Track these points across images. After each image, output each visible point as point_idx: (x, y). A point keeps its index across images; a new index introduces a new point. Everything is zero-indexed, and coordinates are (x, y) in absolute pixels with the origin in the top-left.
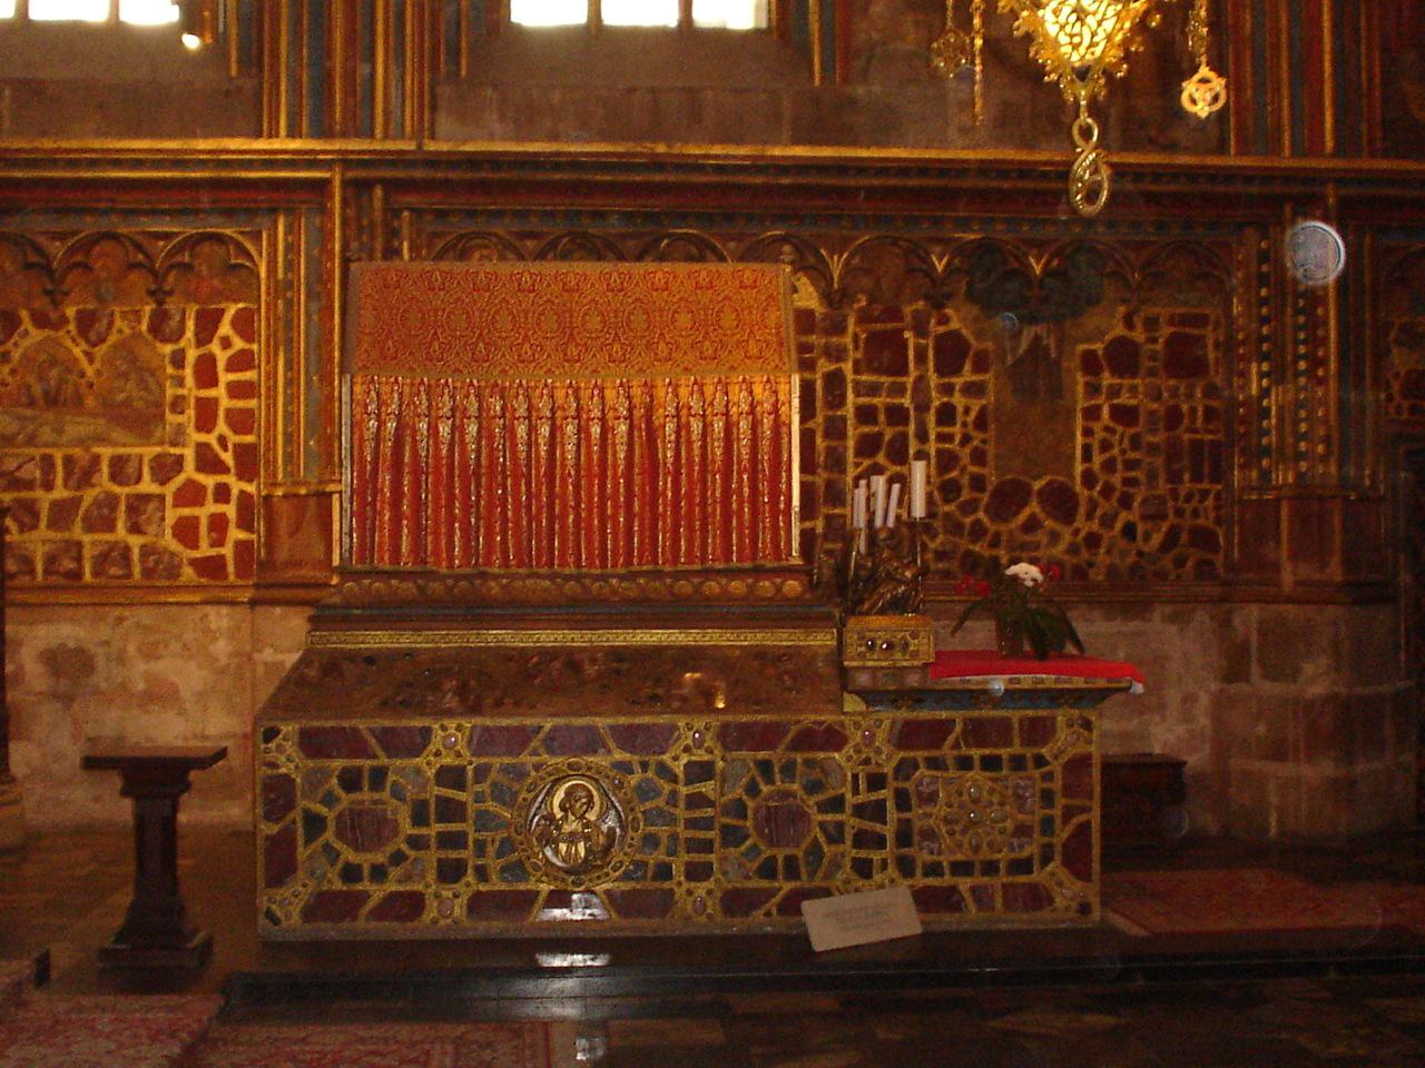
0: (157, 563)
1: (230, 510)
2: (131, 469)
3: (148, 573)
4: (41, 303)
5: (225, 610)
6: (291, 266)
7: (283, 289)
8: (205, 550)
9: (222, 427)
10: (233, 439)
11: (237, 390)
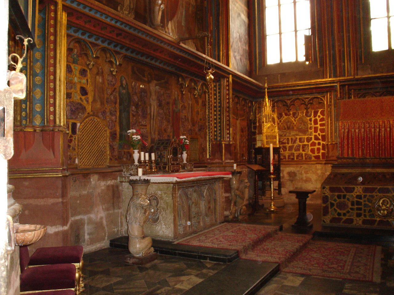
0: (308, 156)
1: (321, 147)
2: (303, 140)
3: (306, 158)
4: (287, 112)
5: (320, 165)
6: (330, 102)
7: (329, 106)
8: (316, 154)
9: (319, 132)
10: (321, 134)
11: (321, 125)
